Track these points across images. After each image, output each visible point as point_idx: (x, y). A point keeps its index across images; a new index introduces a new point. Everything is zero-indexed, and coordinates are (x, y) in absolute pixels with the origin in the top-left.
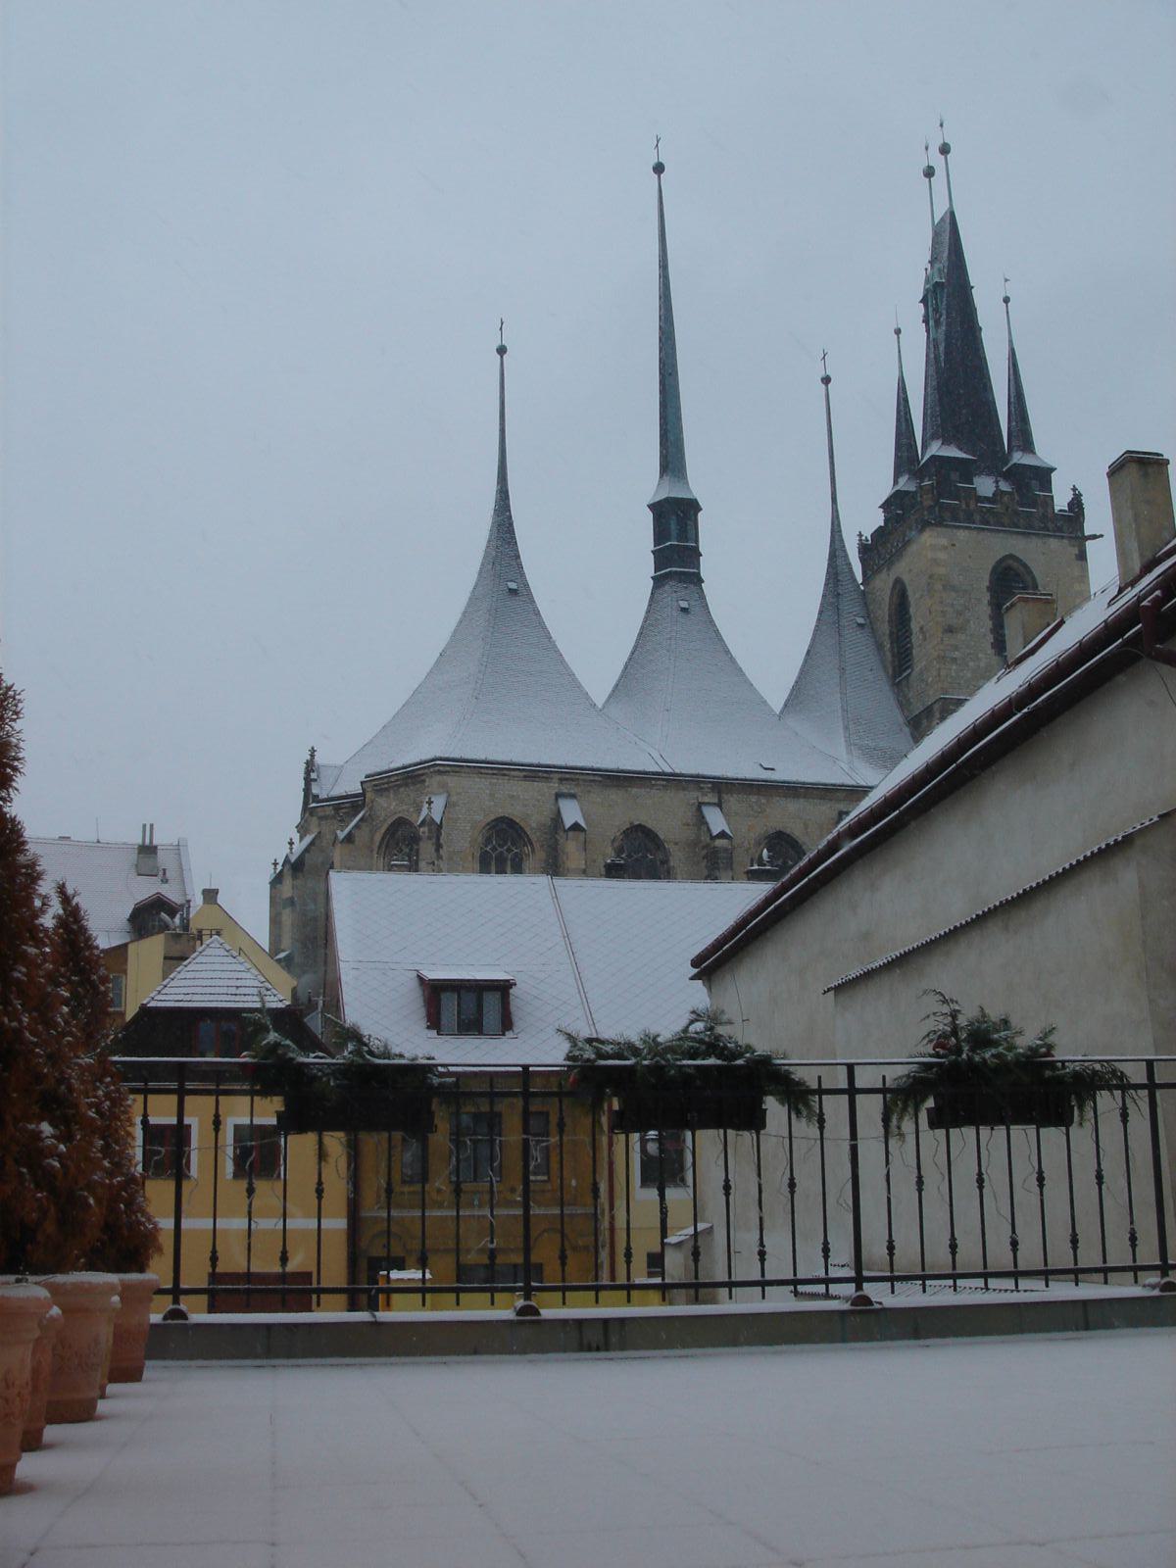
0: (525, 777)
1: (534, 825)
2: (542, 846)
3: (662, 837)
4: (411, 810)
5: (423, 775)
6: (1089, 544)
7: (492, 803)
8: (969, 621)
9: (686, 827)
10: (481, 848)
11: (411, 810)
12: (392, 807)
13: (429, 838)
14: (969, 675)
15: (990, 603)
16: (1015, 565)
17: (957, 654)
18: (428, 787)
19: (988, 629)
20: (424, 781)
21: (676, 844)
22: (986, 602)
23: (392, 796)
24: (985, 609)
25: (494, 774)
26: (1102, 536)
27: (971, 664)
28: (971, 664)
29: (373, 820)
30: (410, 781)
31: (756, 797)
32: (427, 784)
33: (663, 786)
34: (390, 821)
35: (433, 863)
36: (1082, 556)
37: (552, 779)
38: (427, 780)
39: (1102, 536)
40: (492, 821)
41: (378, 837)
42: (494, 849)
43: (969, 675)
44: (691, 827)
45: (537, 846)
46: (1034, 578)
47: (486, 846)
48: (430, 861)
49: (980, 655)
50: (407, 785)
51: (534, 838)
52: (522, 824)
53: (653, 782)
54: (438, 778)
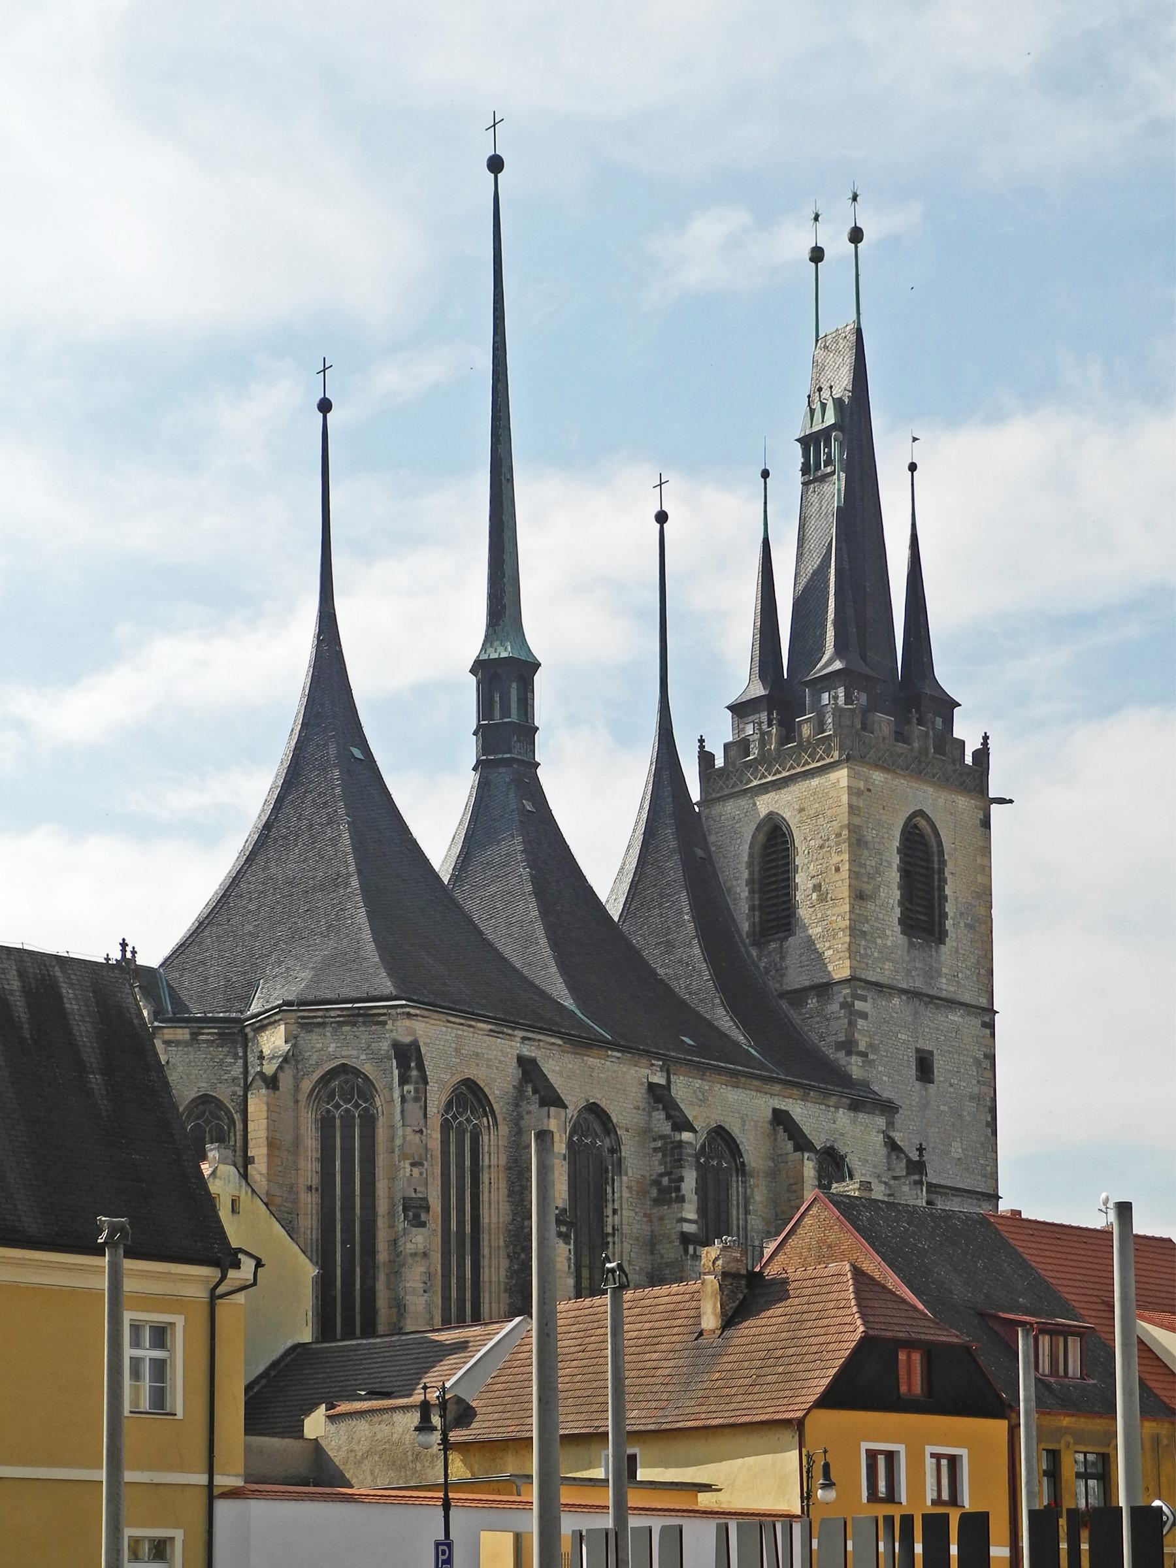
0: (491, 1030)
1: (497, 1092)
2: (504, 1119)
3: (615, 1121)
4: (363, 1057)
5: (384, 1014)
6: (994, 807)
7: (458, 1061)
8: (879, 886)
9: (635, 1111)
10: (443, 1115)
11: (363, 1057)
12: (330, 1049)
13: (417, 1099)
14: (876, 954)
15: (900, 870)
16: (923, 823)
17: (866, 928)
18: (392, 1031)
19: (896, 902)
20: (384, 1023)
21: (627, 1130)
22: (895, 866)
23: (328, 1034)
24: (894, 874)
25: (462, 1024)
26: (1011, 801)
27: (879, 941)
28: (879, 941)
29: (297, 1062)
30: (361, 1019)
31: (700, 1081)
32: (387, 1027)
33: (618, 1058)
34: (327, 1067)
35: (421, 1131)
36: (986, 823)
37: (515, 1036)
38: (390, 1022)
39: (1011, 801)
40: (458, 1083)
41: (307, 1085)
42: (455, 1118)
43: (876, 954)
44: (639, 1112)
45: (499, 1118)
46: (940, 844)
47: (448, 1114)
48: (417, 1129)
49: (888, 932)
50: (354, 1024)
51: (496, 1107)
52: (486, 1090)
53: (610, 1053)
54: (407, 1022)
